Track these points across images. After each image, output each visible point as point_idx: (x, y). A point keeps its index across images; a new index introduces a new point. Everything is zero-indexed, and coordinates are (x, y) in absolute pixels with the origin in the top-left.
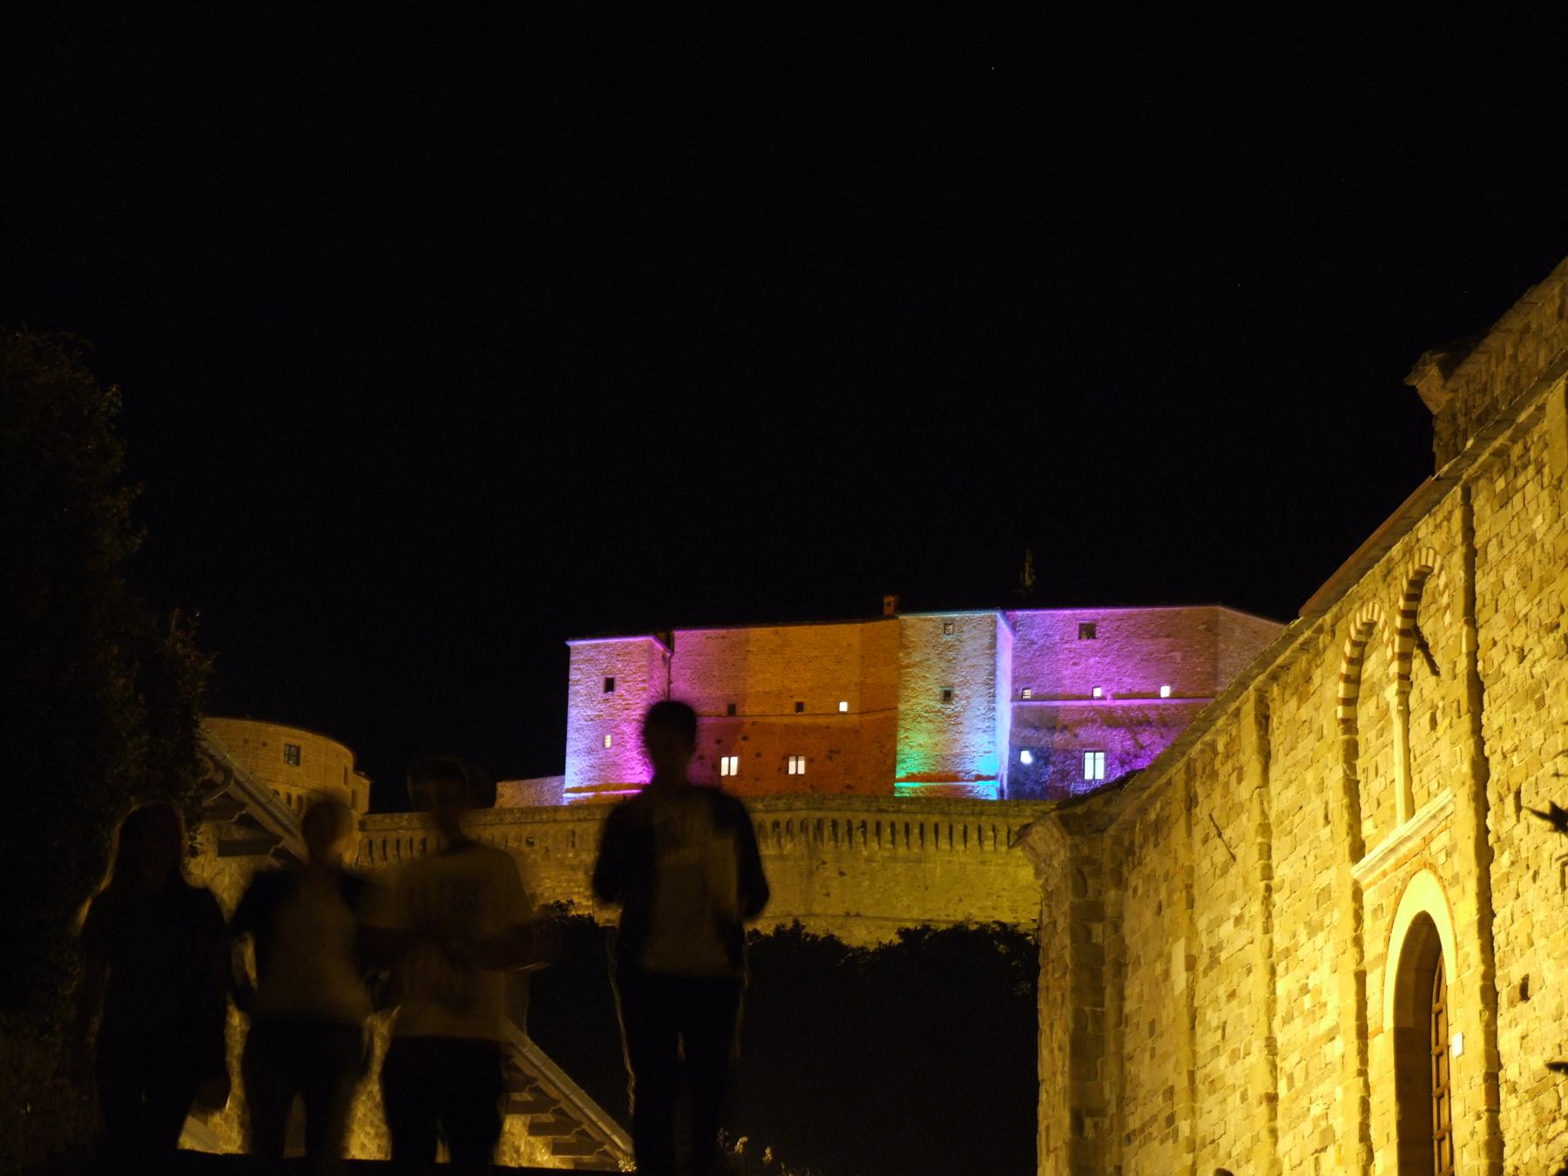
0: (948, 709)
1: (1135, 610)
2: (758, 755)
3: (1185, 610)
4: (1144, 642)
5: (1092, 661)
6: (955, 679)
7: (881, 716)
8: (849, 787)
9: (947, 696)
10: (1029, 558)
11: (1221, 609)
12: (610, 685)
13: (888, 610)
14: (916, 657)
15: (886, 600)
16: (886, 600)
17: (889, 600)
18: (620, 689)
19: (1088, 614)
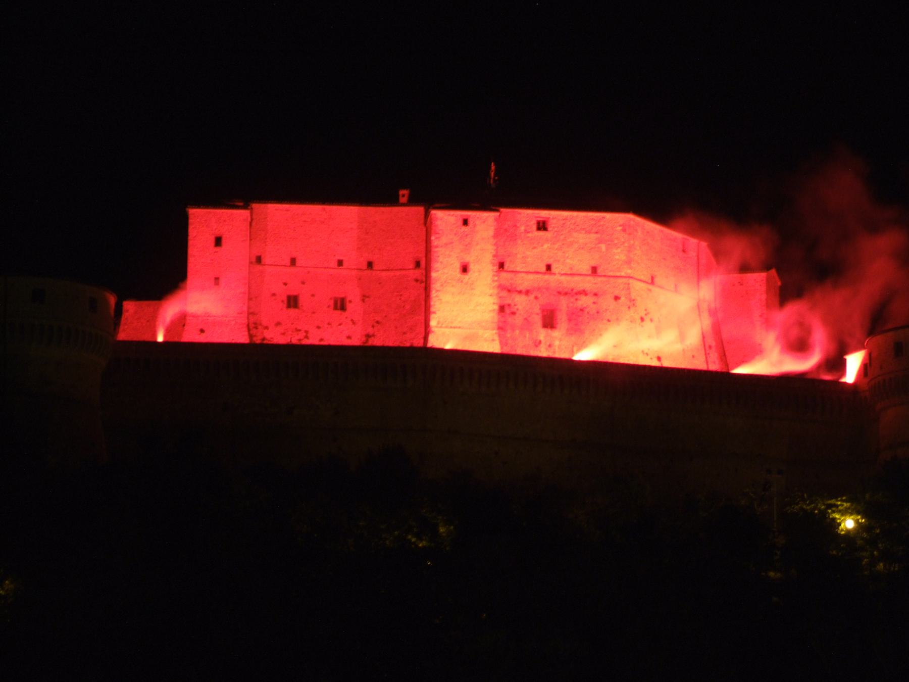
0: (466, 278)
1: (575, 214)
2: (313, 295)
3: (608, 216)
4: (581, 235)
5: (546, 246)
6: (468, 258)
7: (398, 273)
8: (377, 322)
9: (465, 269)
10: (493, 168)
11: (631, 216)
12: (218, 241)
13: (403, 200)
14: (444, 240)
15: (401, 192)
16: (401, 192)
17: (404, 194)
18: (226, 245)
19: (544, 214)
